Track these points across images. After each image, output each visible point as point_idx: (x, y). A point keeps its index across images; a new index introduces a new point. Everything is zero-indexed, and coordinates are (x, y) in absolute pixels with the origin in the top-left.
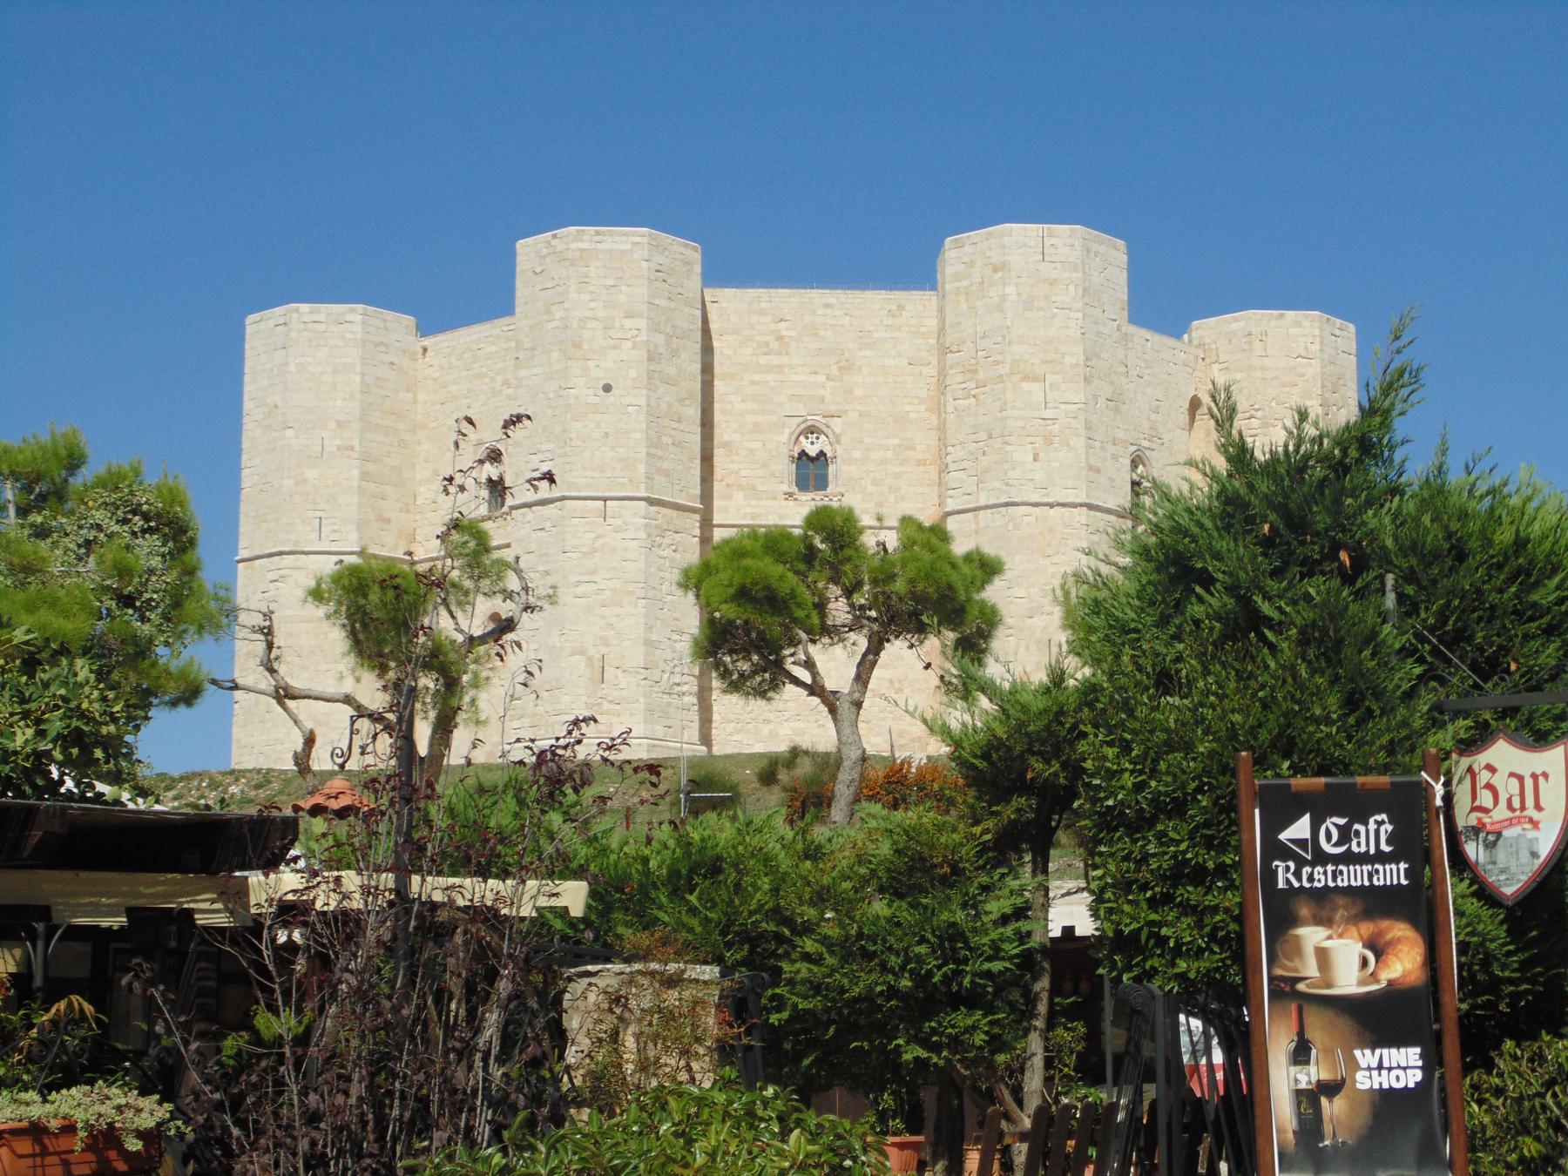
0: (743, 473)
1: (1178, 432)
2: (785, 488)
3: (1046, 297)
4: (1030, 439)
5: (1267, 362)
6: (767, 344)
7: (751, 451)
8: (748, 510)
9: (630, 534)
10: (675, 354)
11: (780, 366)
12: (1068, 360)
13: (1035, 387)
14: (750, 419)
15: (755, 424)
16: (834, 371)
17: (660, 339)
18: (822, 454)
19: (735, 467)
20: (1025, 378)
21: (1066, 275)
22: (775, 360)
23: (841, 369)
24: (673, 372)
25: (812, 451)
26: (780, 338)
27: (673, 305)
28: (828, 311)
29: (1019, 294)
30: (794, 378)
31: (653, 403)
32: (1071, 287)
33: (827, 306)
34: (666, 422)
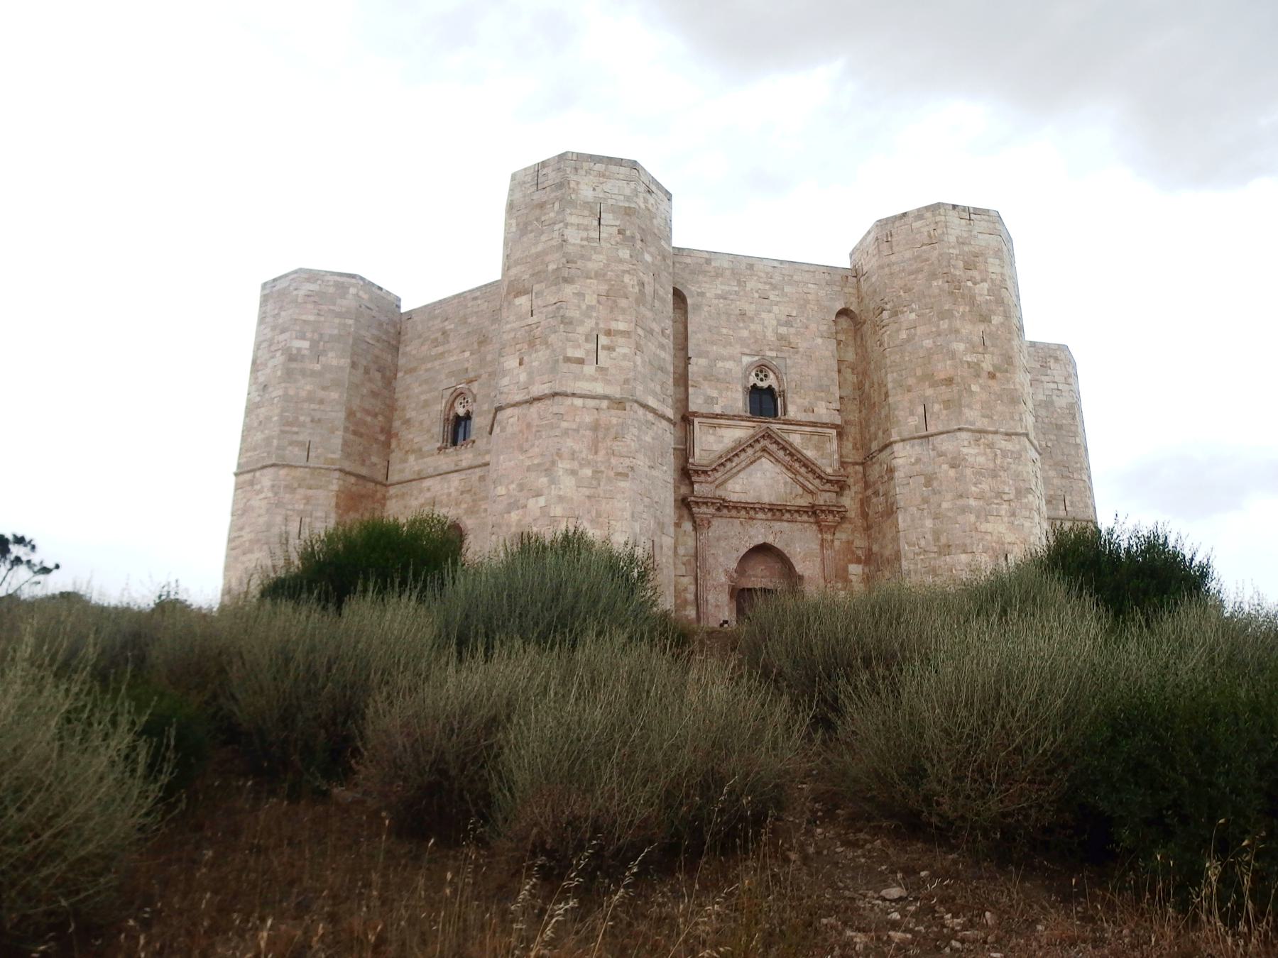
0: (416, 440)
1: (819, 341)
2: (439, 445)
3: (537, 220)
4: (518, 347)
5: (893, 258)
6: (436, 339)
7: (421, 423)
8: (416, 468)
9: (262, 496)
10: (317, 355)
11: (442, 354)
12: (552, 267)
13: (523, 301)
14: (423, 397)
15: (426, 401)
16: (476, 346)
17: (306, 344)
18: (468, 416)
19: (411, 436)
20: (519, 294)
21: (553, 195)
22: (440, 349)
23: (481, 343)
24: (318, 367)
25: (461, 411)
26: (444, 333)
27: (322, 319)
28: (475, 303)
29: (518, 225)
30: (452, 359)
31: (291, 392)
32: (557, 205)
33: (475, 299)
34: (306, 405)
